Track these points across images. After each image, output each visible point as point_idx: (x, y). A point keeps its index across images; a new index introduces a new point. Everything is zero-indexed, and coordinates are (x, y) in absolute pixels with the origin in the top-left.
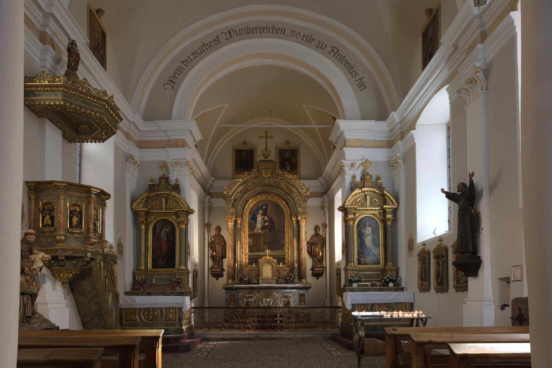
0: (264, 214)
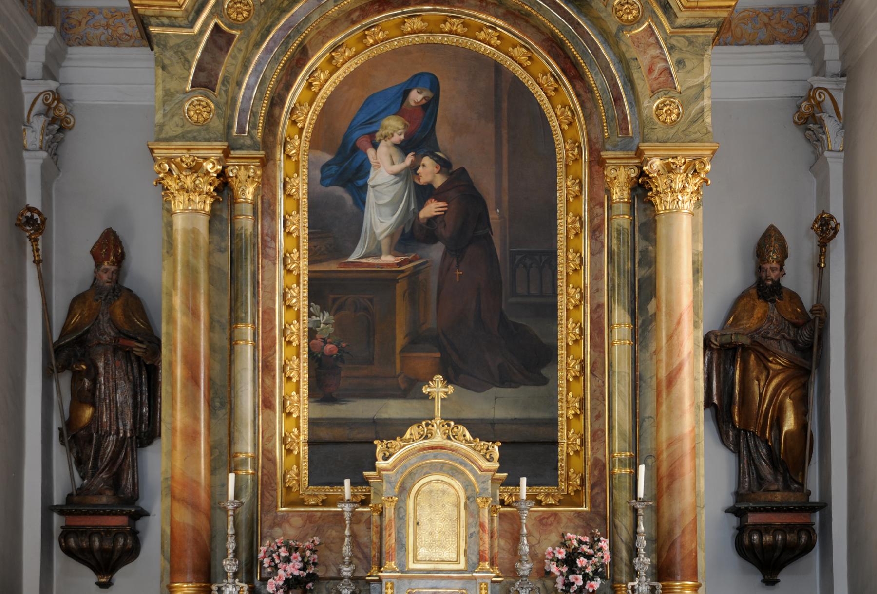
0: (417, 143)
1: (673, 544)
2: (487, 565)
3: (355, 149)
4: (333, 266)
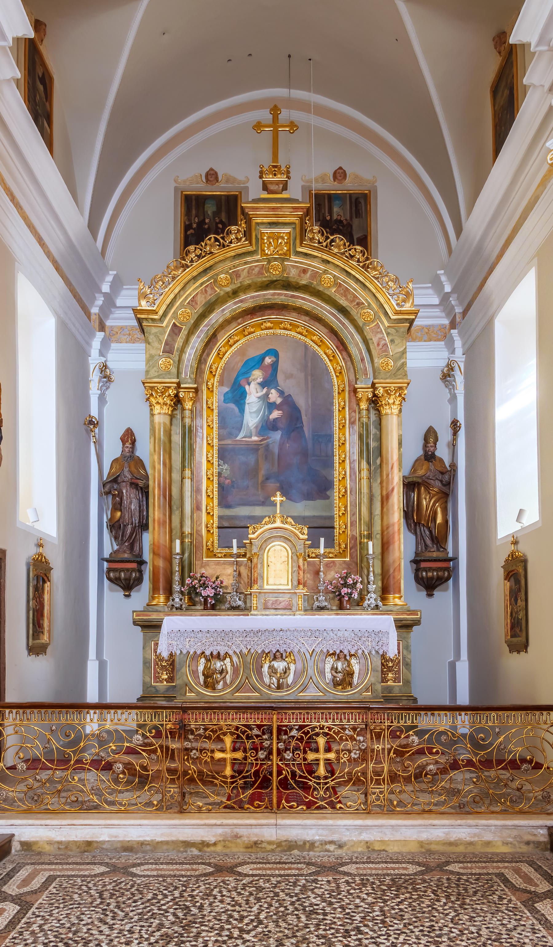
1: (389, 576)
2: (301, 586)
3: (240, 385)
4: (229, 442)
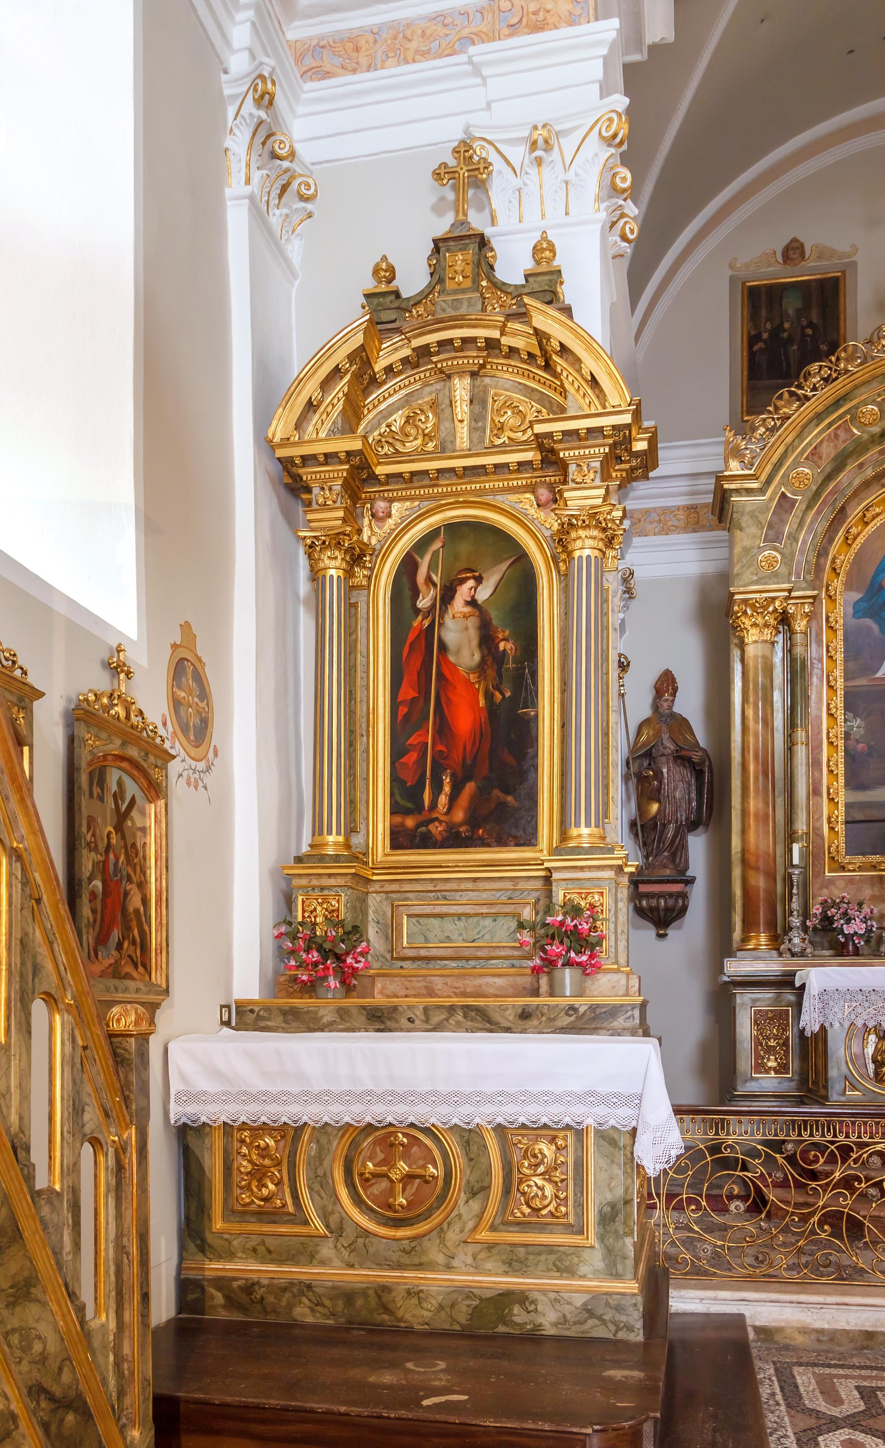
4: (863, 682)
